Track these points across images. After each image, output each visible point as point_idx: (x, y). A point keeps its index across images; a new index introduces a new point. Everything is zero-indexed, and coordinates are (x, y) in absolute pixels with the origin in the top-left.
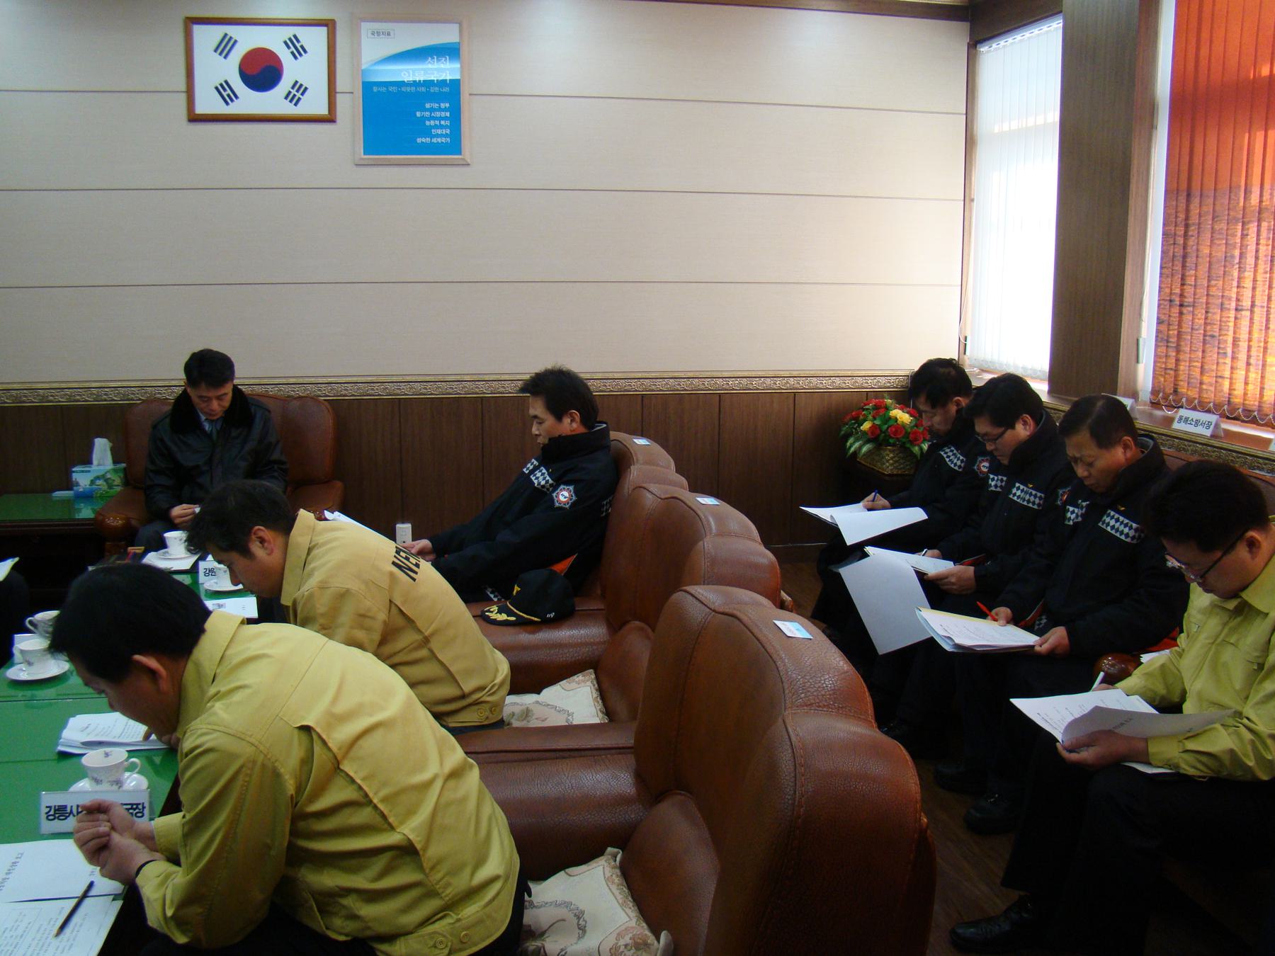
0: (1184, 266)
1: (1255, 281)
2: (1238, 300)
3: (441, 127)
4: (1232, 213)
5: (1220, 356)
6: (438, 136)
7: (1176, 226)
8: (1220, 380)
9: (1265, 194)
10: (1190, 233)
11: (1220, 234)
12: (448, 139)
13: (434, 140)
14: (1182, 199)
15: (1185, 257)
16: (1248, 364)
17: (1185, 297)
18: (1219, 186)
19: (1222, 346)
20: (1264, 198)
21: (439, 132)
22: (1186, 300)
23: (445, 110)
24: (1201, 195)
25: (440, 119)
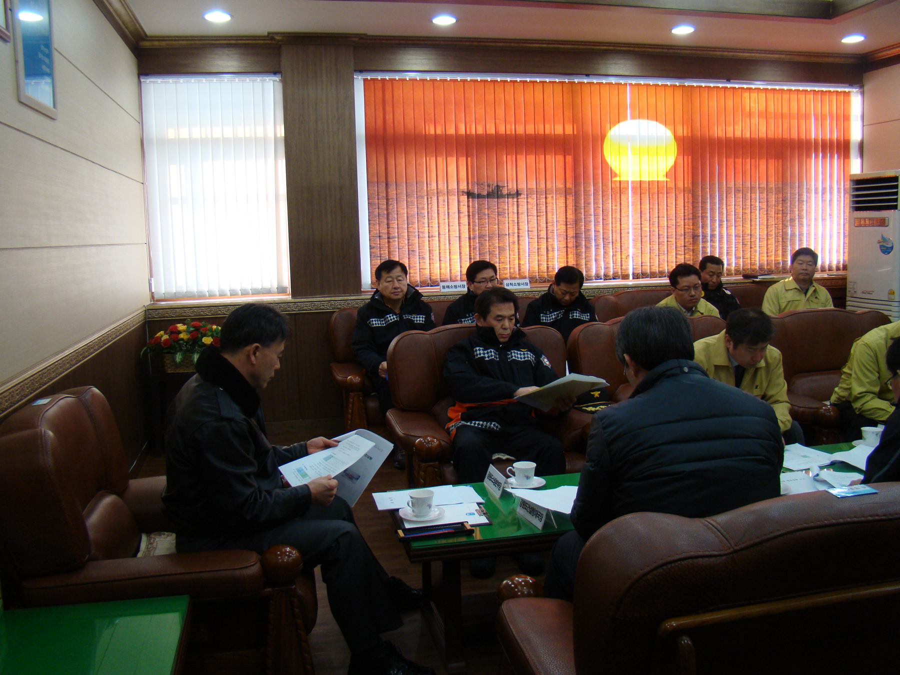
0: (388, 219)
1: (439, 223)
2: (429, 233)
4: (418, 193)
5: (420, 259)
7: (378, 200)
8: (421, 270)
9: (439, 185)
10: (390, 203)
11: (412, 203)
14: (382, 187)
15: (388, 214)
16: (440, 260)
17: (390, 234)
18: (408, 181)
19: (420, 254)
20: (439, 187)
22: (391, 235)
24: (396, 185)
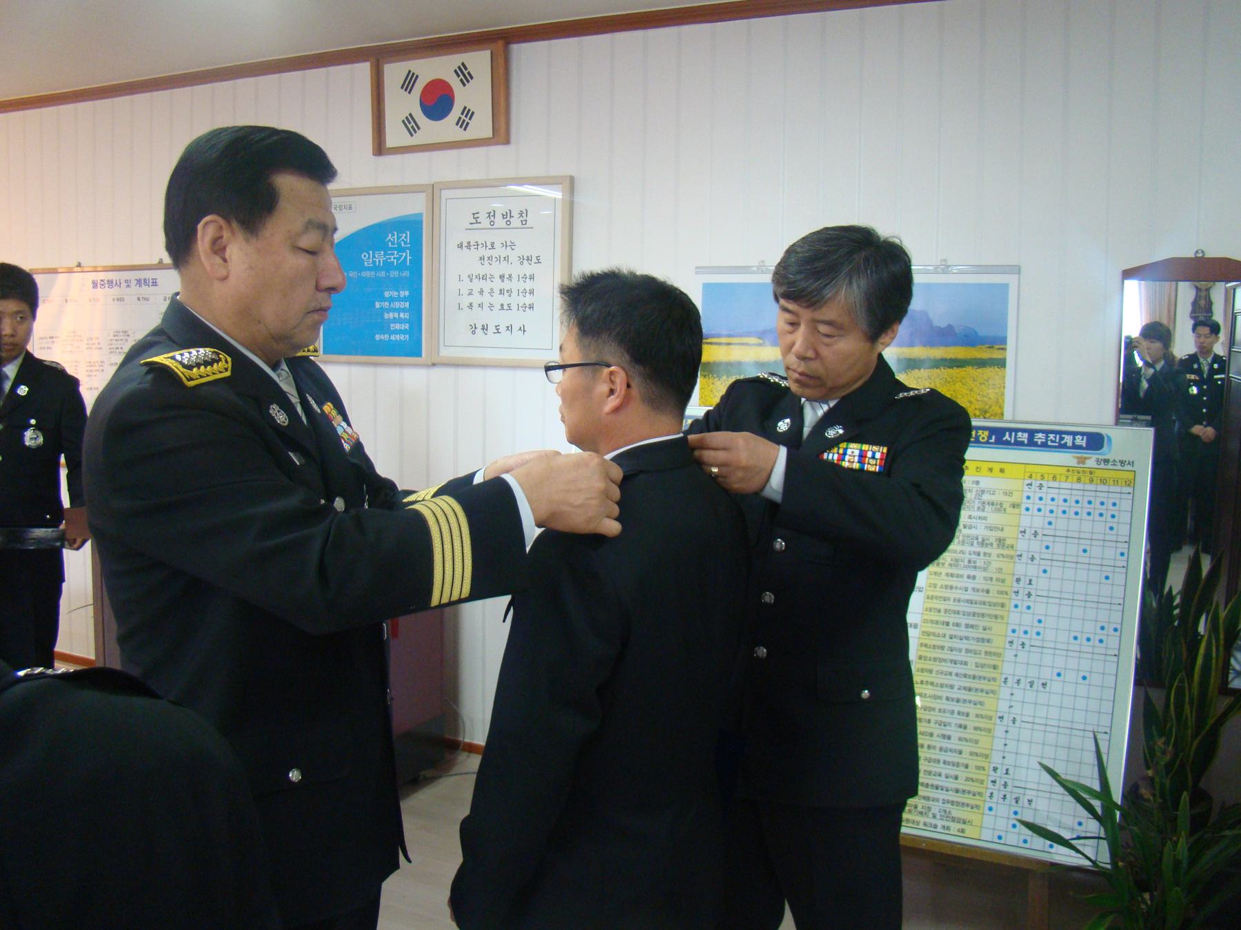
3: (401, 321)
6: (396, 332)
12: (407, 336)
13: (393, 338)
21: (398, 326)
23: (405, 299)
25: (399, 310)
